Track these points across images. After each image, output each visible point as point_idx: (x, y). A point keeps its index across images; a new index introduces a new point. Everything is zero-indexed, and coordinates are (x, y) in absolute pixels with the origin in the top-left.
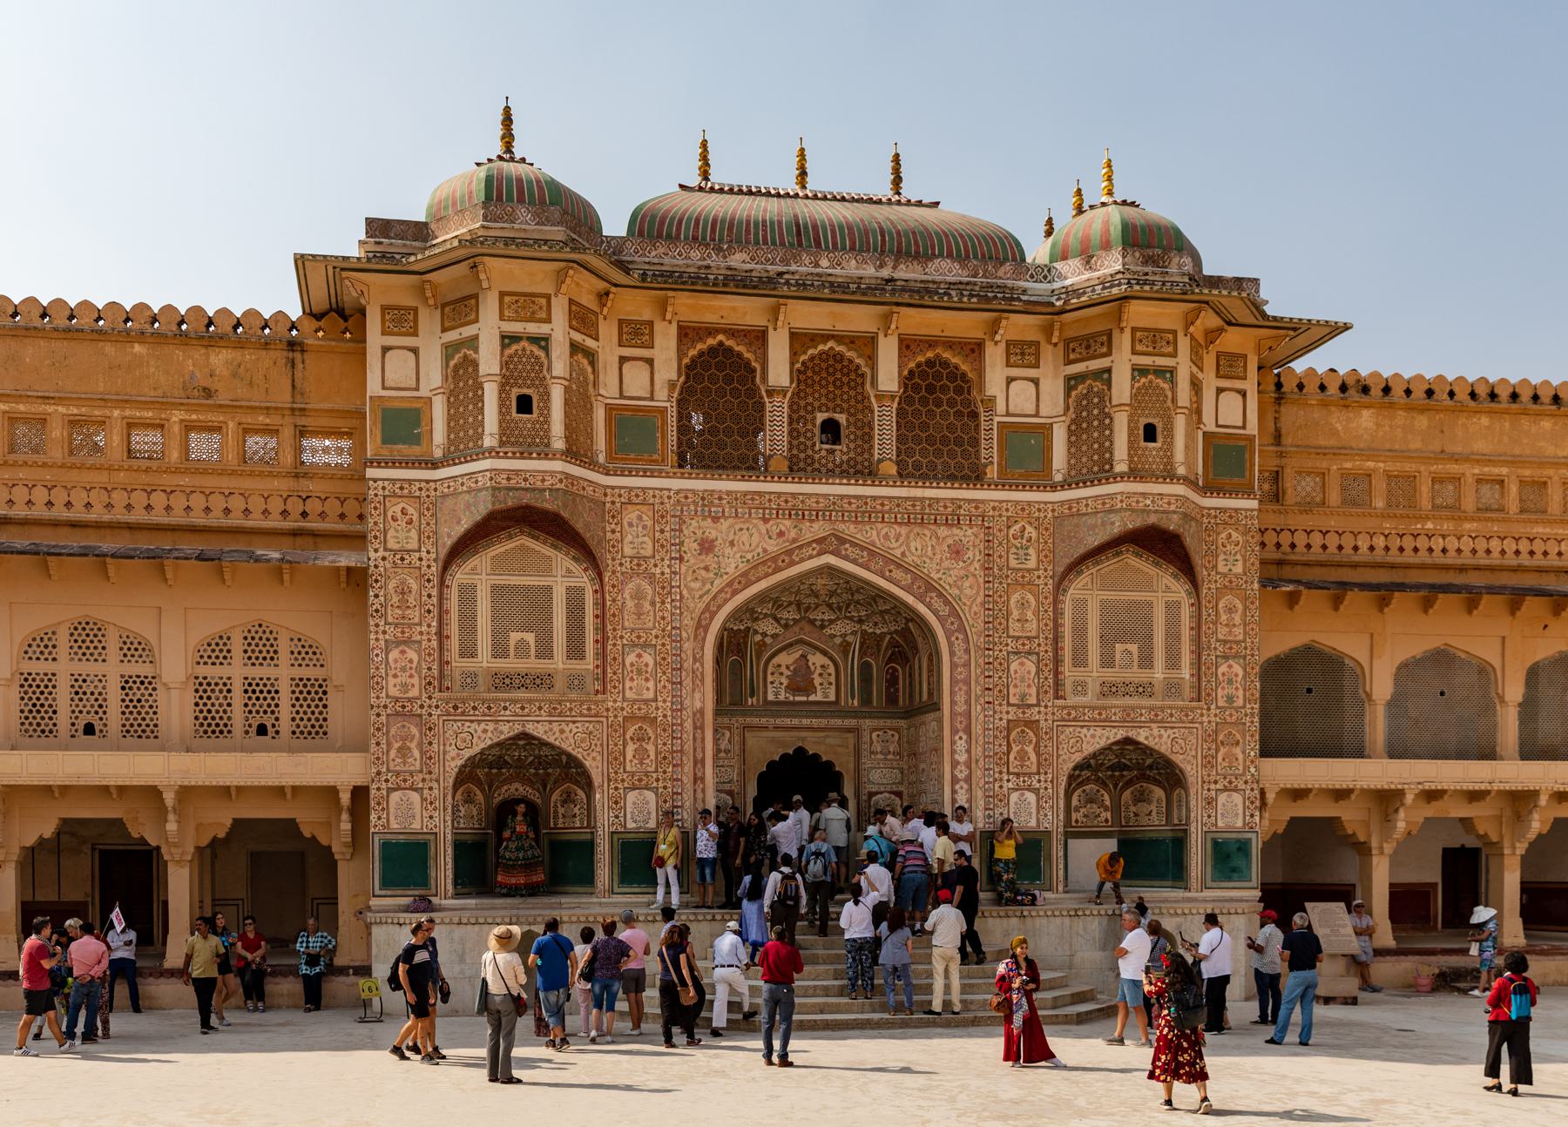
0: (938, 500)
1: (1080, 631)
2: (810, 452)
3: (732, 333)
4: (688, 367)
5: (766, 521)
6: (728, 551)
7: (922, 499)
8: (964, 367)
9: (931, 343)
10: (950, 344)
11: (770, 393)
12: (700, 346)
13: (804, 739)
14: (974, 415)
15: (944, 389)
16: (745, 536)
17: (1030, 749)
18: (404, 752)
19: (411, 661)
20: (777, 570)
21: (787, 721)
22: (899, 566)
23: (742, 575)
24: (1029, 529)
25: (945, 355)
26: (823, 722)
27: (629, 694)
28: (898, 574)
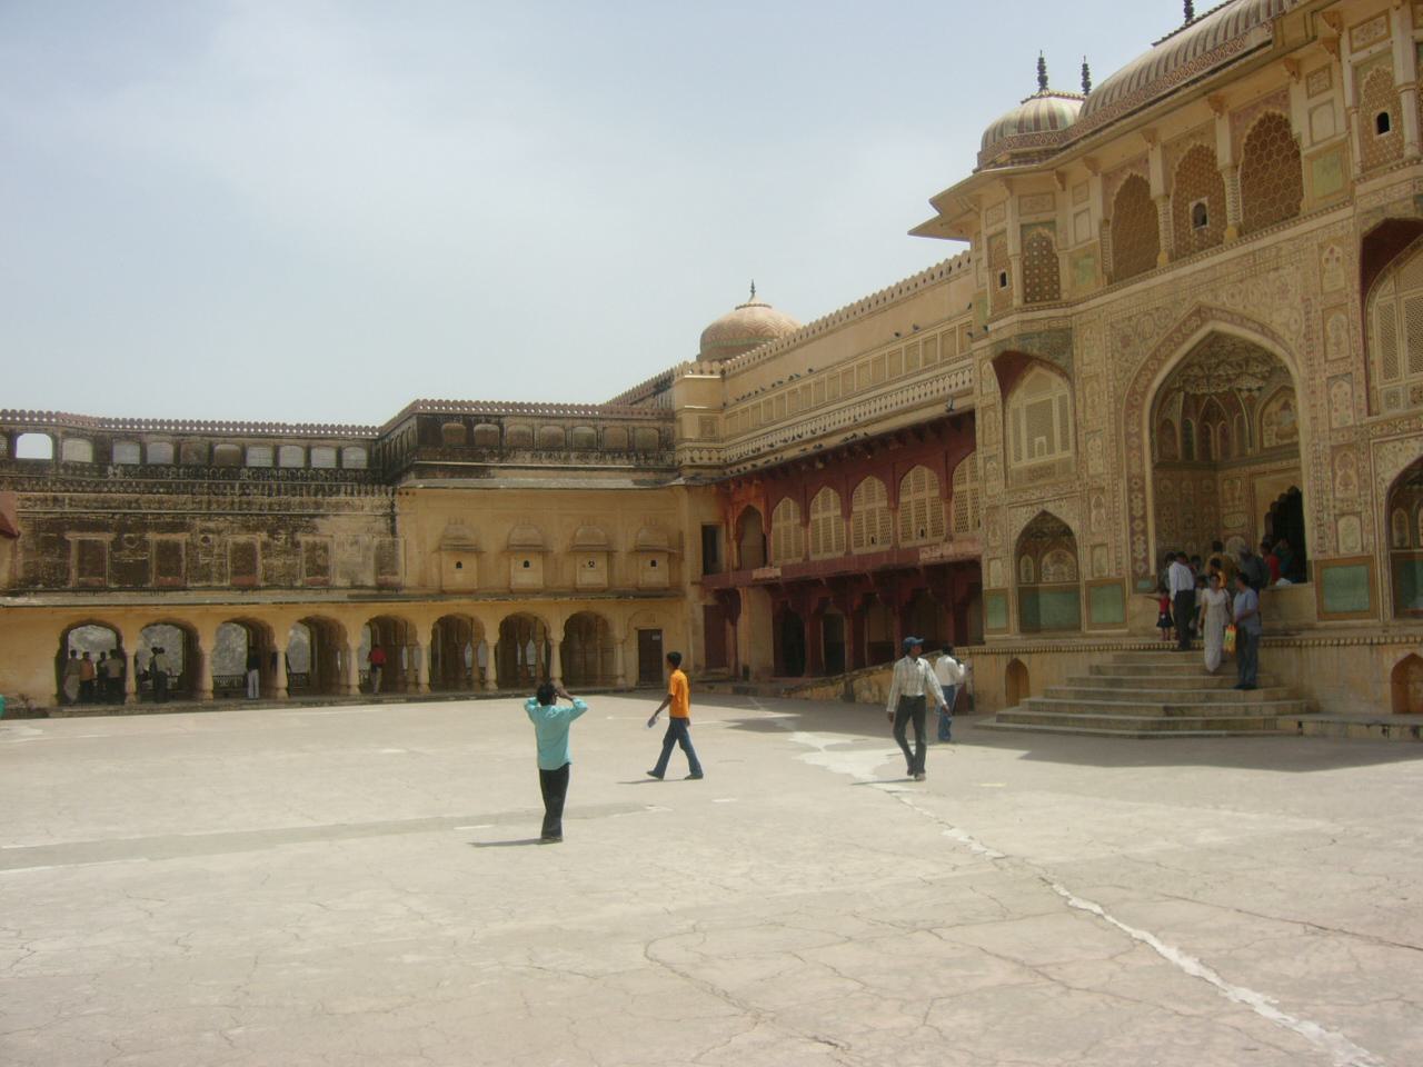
1: (1389, 340)
3: (1132, 165)
4: (1116, 202)
7: (1253, 253)
8: (1284, 114)
12: (1121, 183)
15: (1273, 141)
17: (1352, 472)
18: (994, 535)
19: (994, 469)
20: (1178, 345)
22: (1248, 320)
24: (1337, 249)
25: (1271, 111)
27: (1091, 472)
28: (1250, 324)
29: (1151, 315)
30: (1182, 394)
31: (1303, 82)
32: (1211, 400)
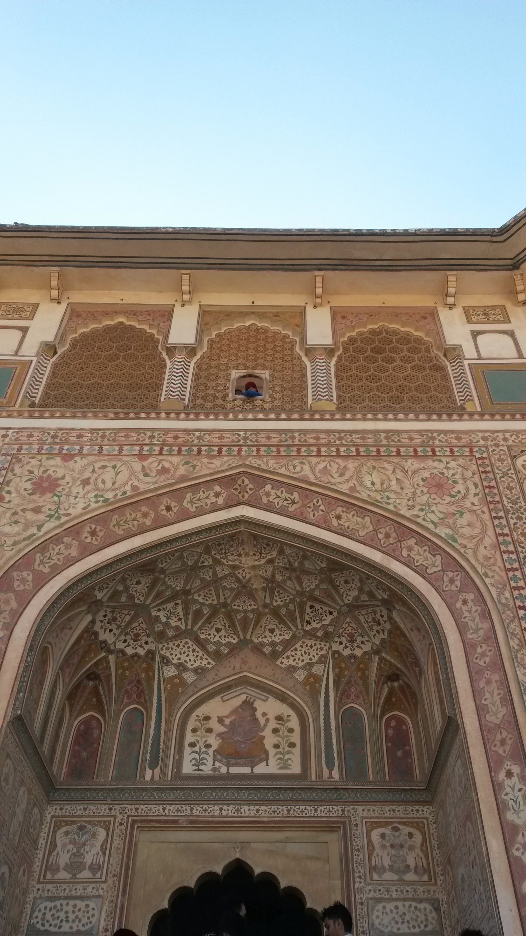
0: (398, 432)
2: (220, 402)
5: (141, 457)
6: (77, 489)
7: (376, 432)
9: (372, 313)
10: (395, 313)
11: (171, 350)
13: (244, 844)
14: (441, 369)
15: (394, 350)
16: (108, 475)
21: (214, 810)
23: (97, 519)
26: (280, 811)
28: (350, 520)
29: (125, 463)
30: (89, 618)
31: (458, 312)
32: (105, 658)
